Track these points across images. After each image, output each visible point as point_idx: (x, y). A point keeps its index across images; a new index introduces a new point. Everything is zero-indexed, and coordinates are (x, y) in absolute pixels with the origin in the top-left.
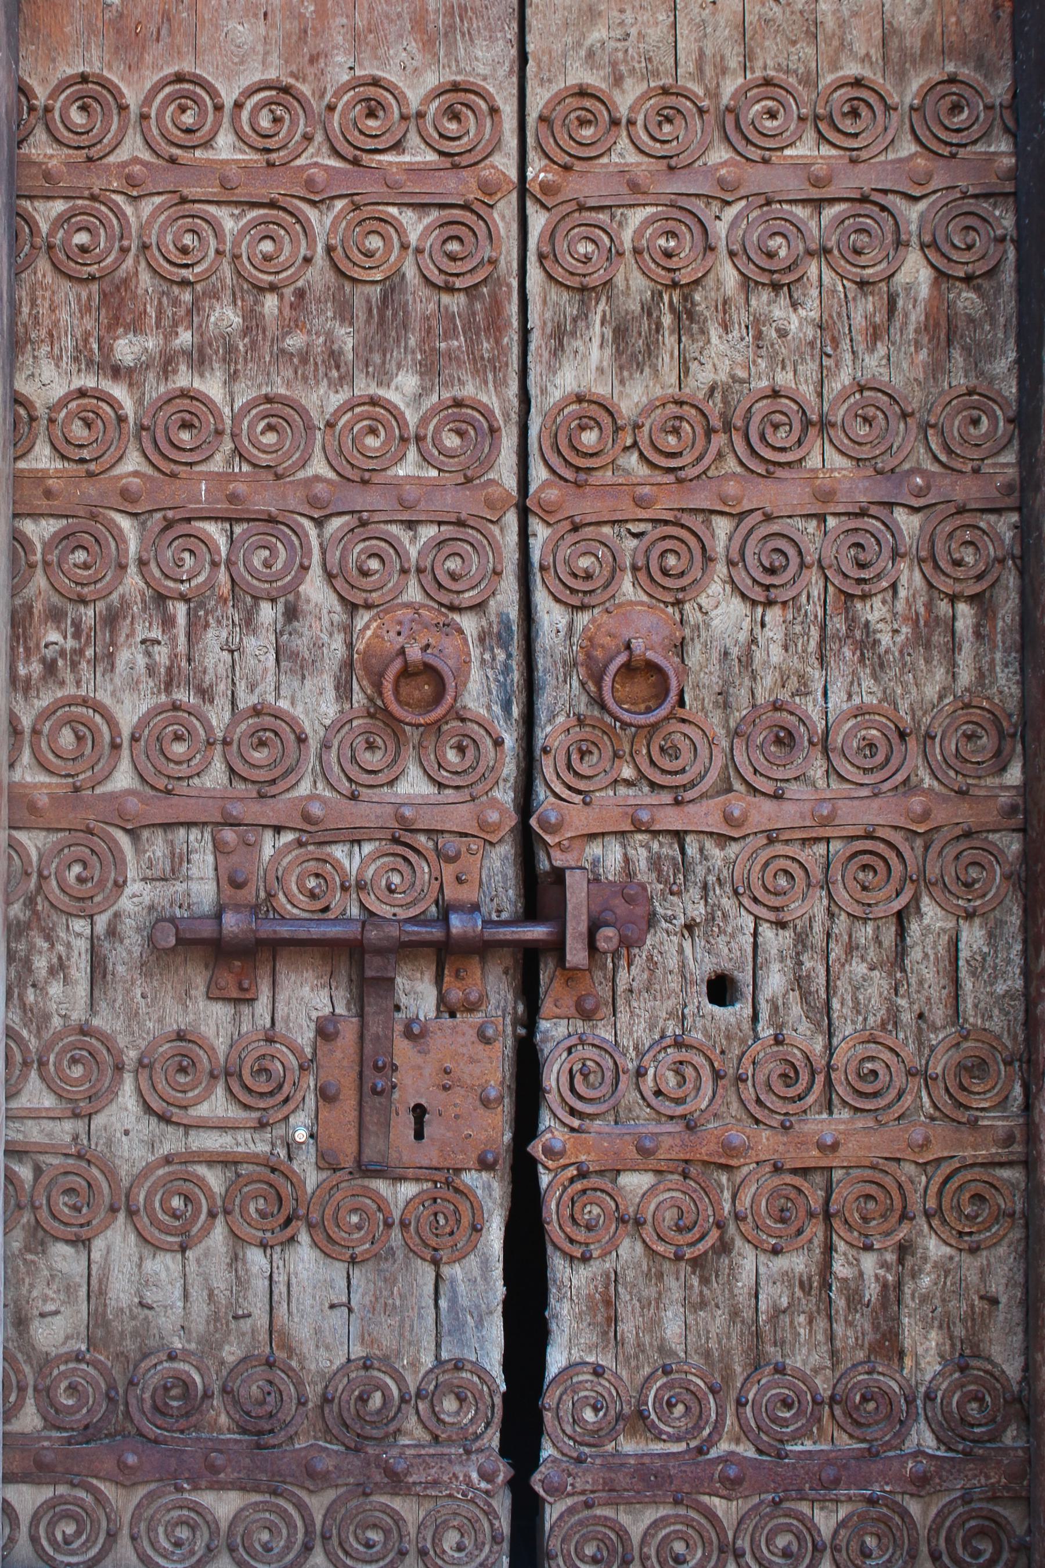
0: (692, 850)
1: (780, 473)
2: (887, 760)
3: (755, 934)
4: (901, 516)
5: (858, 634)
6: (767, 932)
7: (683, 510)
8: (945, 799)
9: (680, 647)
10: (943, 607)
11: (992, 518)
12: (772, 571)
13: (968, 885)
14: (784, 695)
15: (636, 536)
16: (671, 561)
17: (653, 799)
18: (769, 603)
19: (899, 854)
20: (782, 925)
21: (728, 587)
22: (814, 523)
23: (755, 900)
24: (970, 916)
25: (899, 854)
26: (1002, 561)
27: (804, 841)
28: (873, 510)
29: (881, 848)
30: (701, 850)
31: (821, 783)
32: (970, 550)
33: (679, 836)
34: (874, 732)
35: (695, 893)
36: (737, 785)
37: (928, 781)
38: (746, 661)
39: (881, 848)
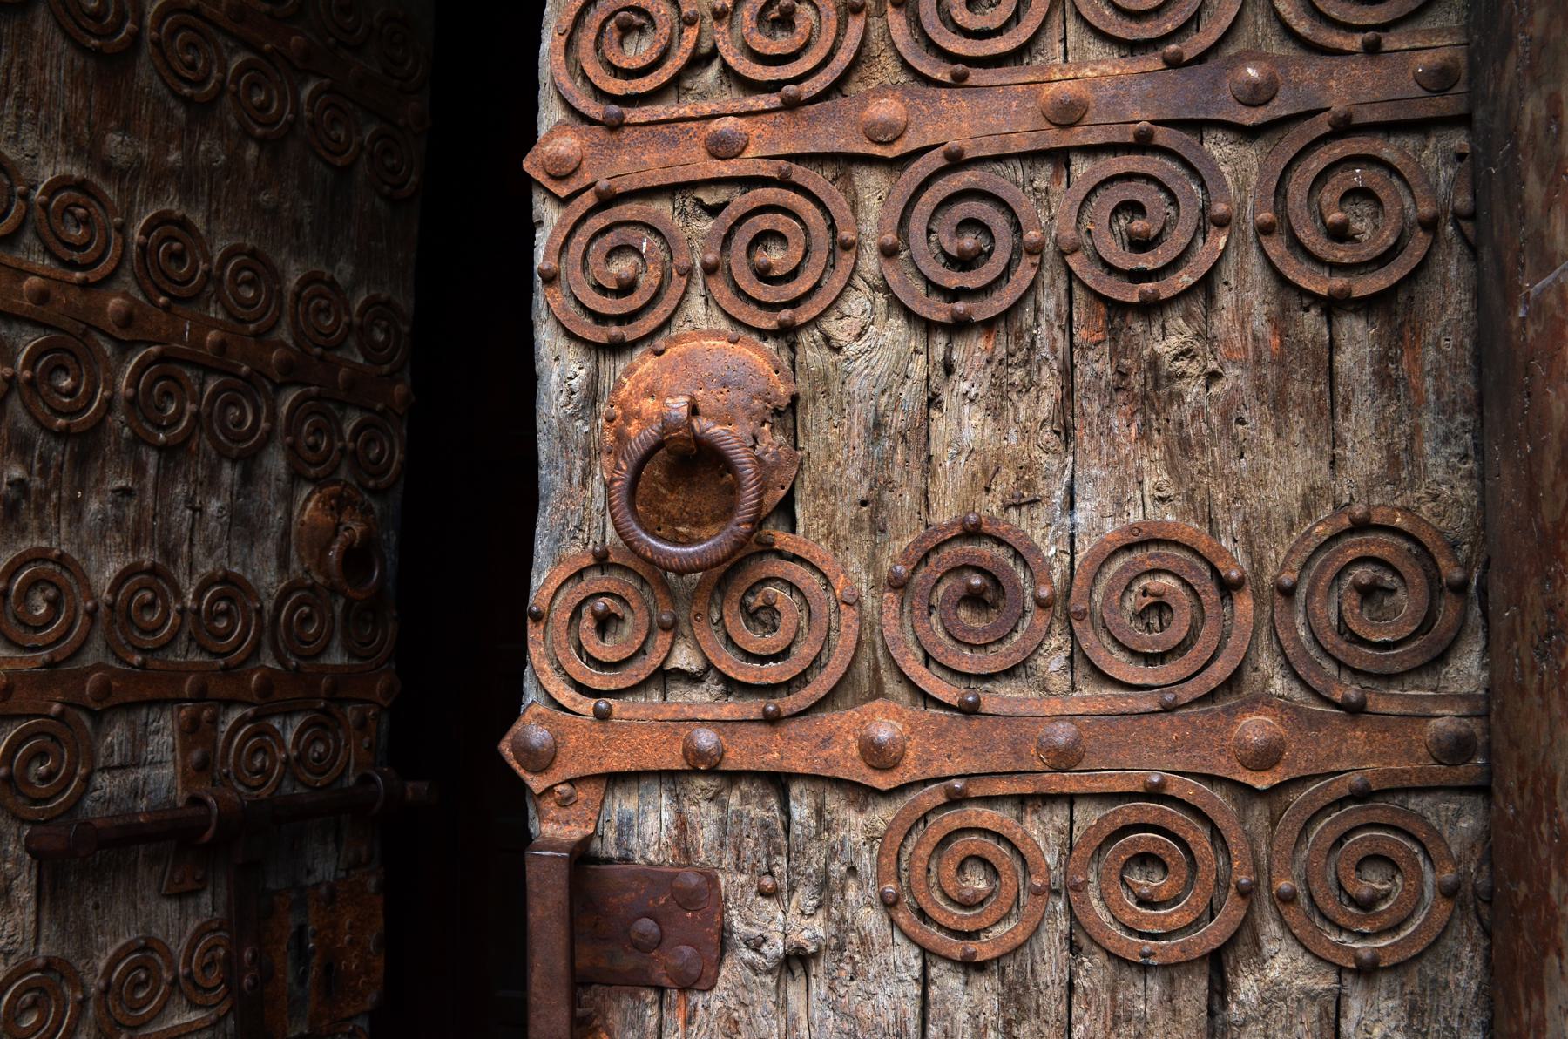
0: (801, 811)
1: (977, 76)
2: (1193, 632)
3: (925, 981)
4: (1218, 148)
5: (1136, 381)
6: (948, 982)
7: (789, 158)
8: (1315, 722)
9: (787, 414)
10: (1311, 323)
11: (1411, 142)
12: (964, 262)
13: (1367, 905)
14: (989, 506)
15: (714, 211)
16: (775, 256)
17: (732, 708)
18: (959, 327)
19: (1216, 834)
20: (971, 967)
21: (881, 299)
22: (1047, 170)
23: (922, 914)
24: (1367, 971)
25: (1216, 834)
26: (1430, 225)
27: (1021, 801)
28: (1163, 136)
29: (1177, 819)
30: (819, 812)
31: (1059, 683)
32: (1365, 208)
33: (779, 782)
34: (1167, 581)
35: (804, 897)
36: (892, 685)
37: (1279, 685)
38: (920, 434)
39: (1177, 819)
